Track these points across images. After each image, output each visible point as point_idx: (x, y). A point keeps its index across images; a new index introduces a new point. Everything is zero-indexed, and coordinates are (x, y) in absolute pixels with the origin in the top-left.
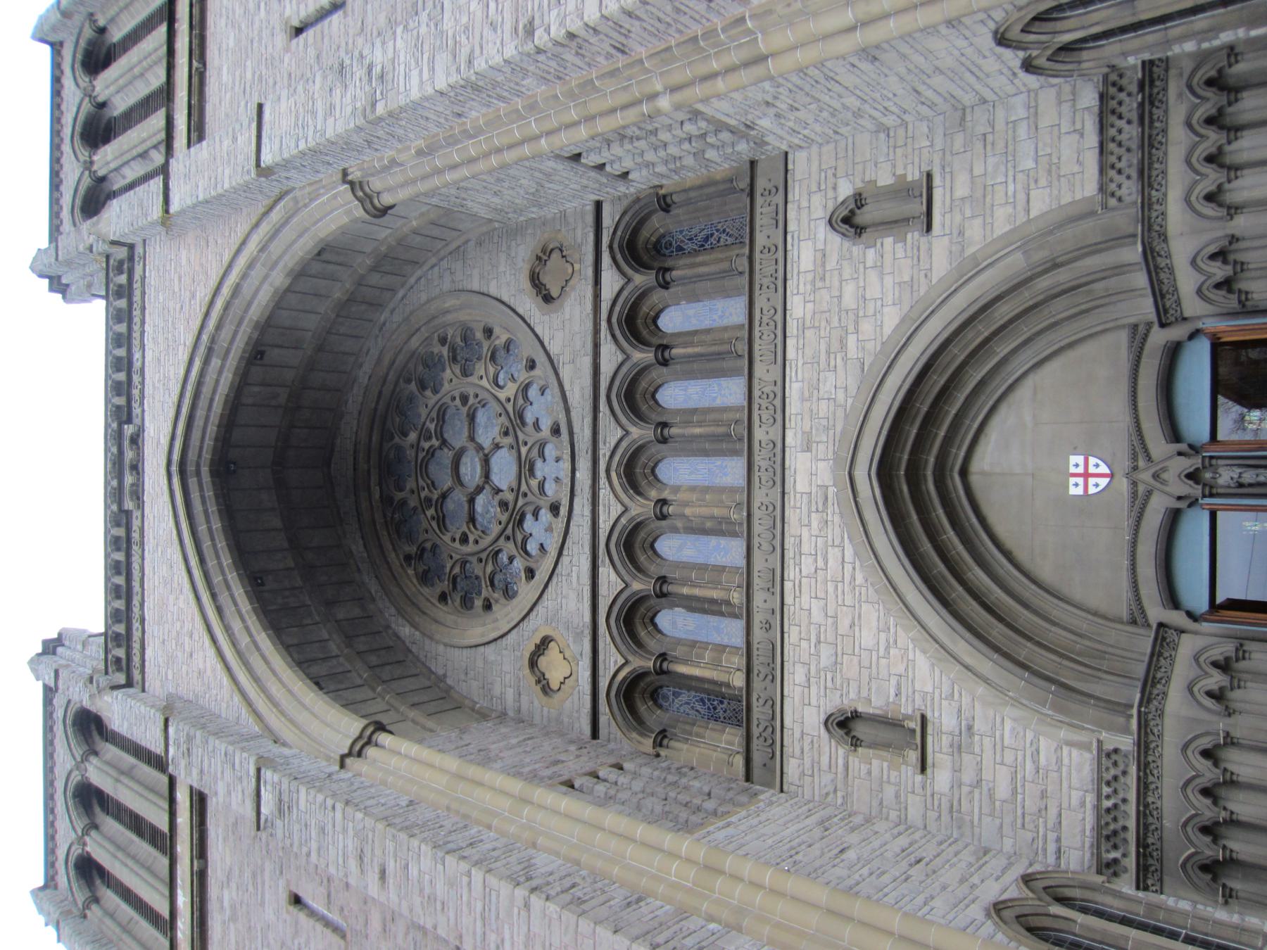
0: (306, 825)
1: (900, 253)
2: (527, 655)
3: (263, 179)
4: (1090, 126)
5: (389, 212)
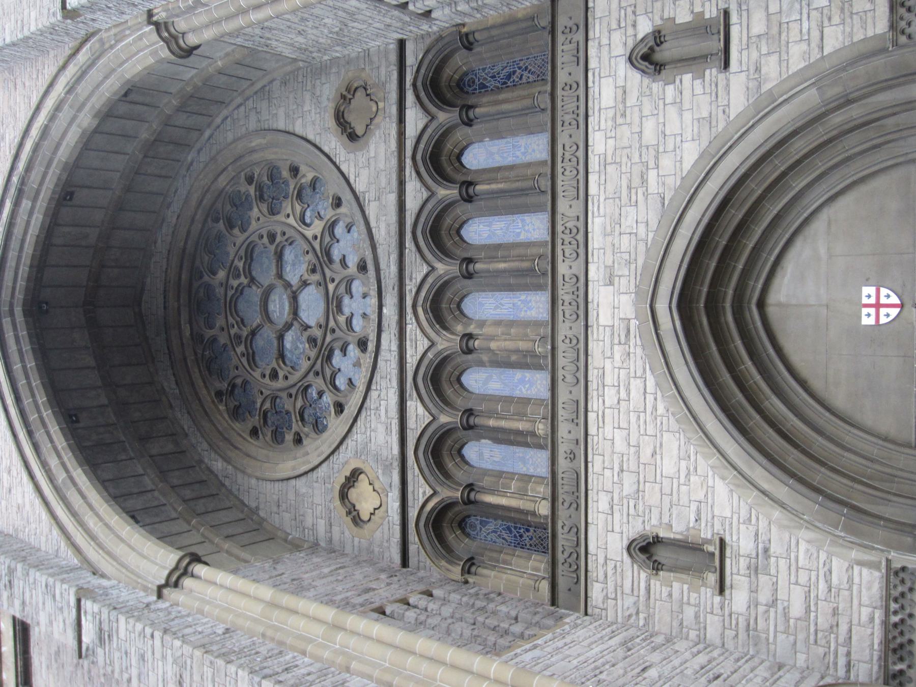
0: (126, 653)
1: (698, 89)
2: (338, 487)
3: (69, 21)
5: (195, 52)
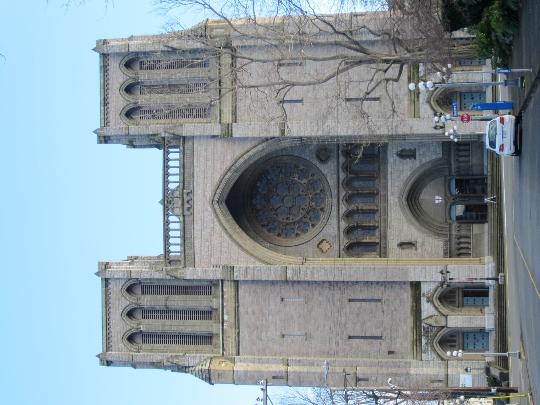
4: (441, 147)
